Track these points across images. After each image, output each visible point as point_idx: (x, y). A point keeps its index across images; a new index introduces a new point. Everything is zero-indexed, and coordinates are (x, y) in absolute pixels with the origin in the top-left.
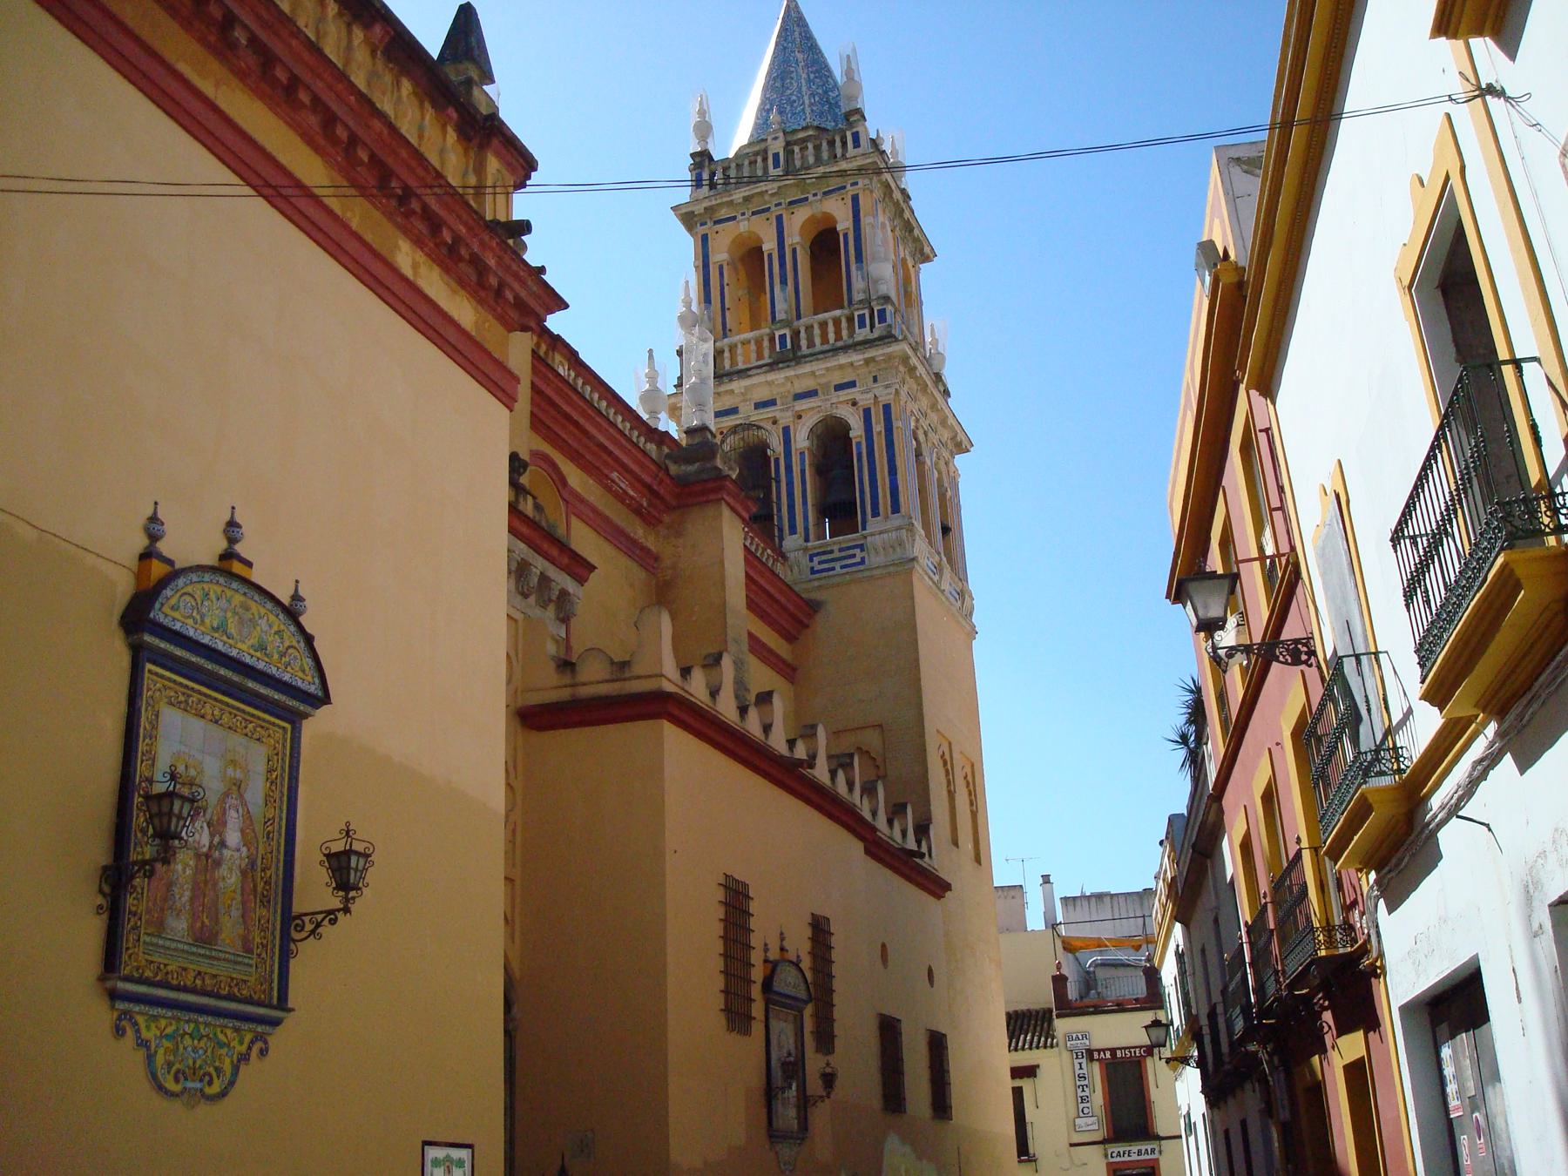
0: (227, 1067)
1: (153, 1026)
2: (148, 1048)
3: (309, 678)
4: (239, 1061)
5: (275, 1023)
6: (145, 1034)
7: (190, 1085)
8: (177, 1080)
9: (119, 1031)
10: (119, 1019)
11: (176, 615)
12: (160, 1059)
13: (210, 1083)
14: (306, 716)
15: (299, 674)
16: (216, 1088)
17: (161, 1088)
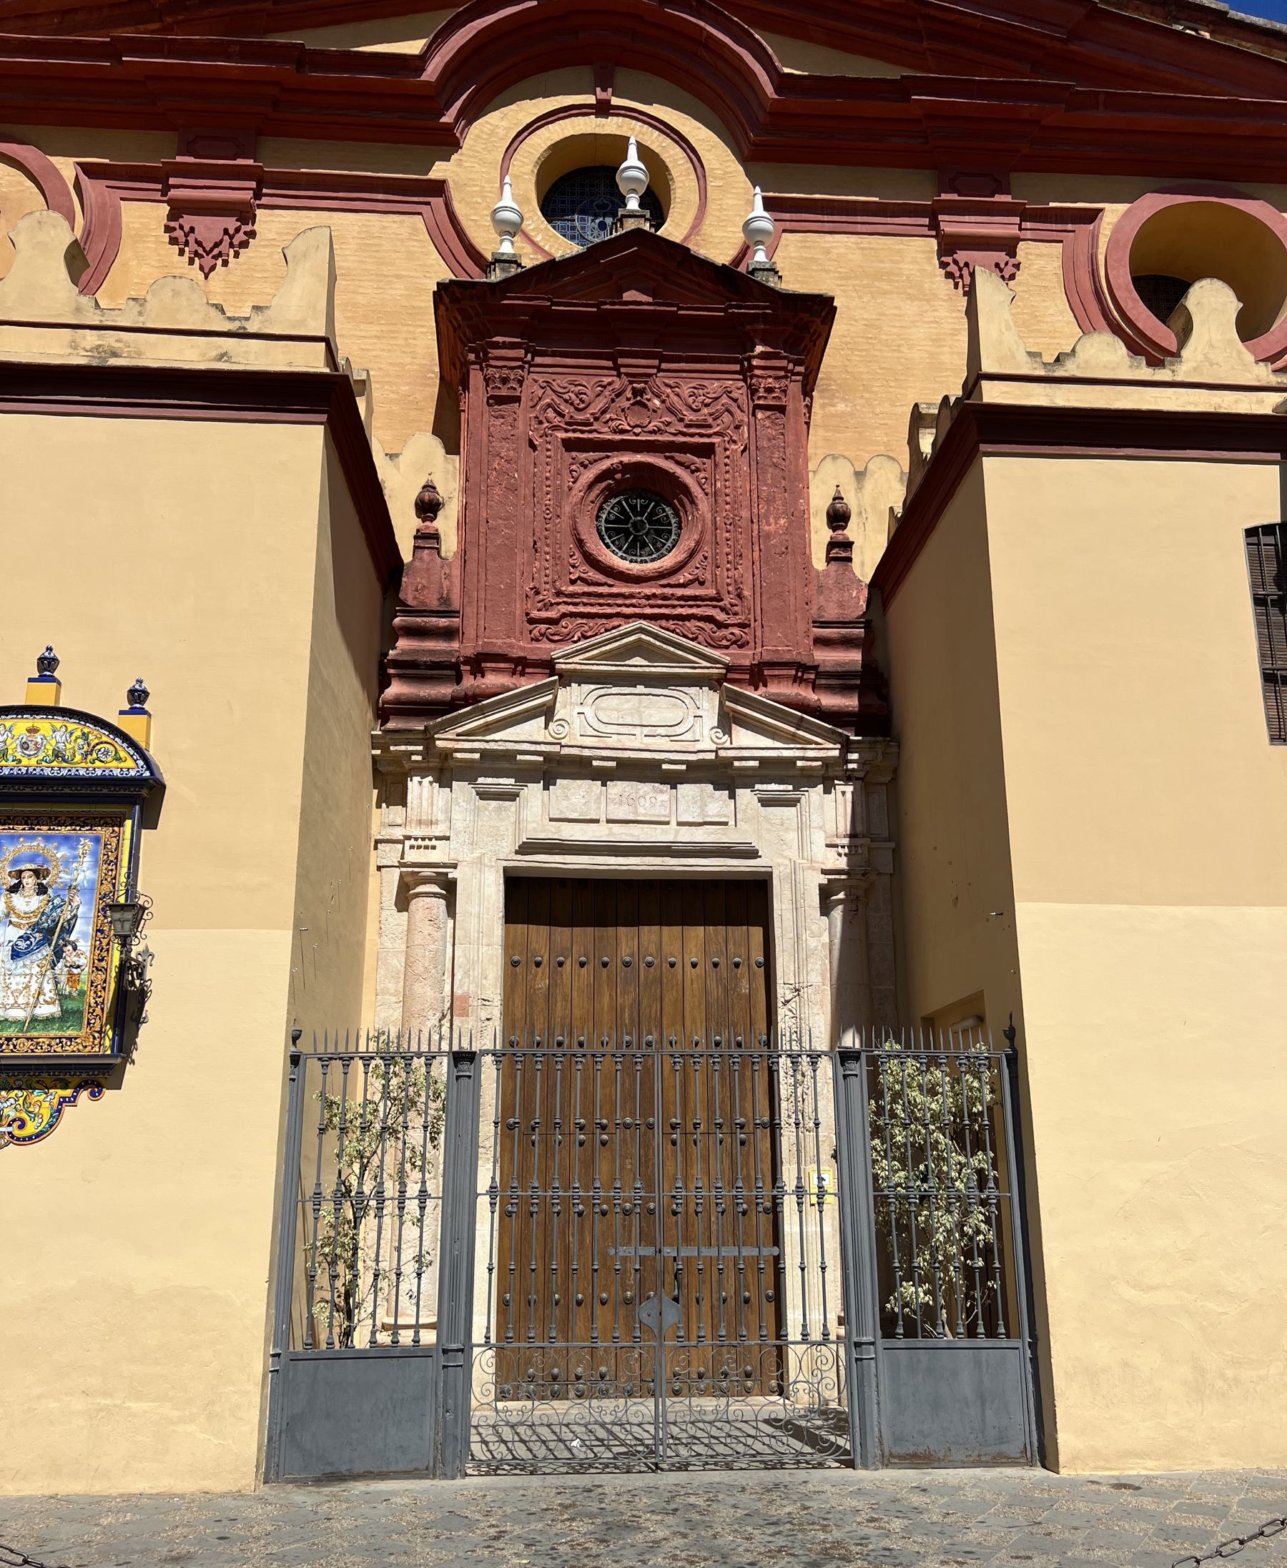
0: (46, 1113)
3: (130, 763)
4: (60, 1104)
13: (21, 1127)
16: (31, 1128)
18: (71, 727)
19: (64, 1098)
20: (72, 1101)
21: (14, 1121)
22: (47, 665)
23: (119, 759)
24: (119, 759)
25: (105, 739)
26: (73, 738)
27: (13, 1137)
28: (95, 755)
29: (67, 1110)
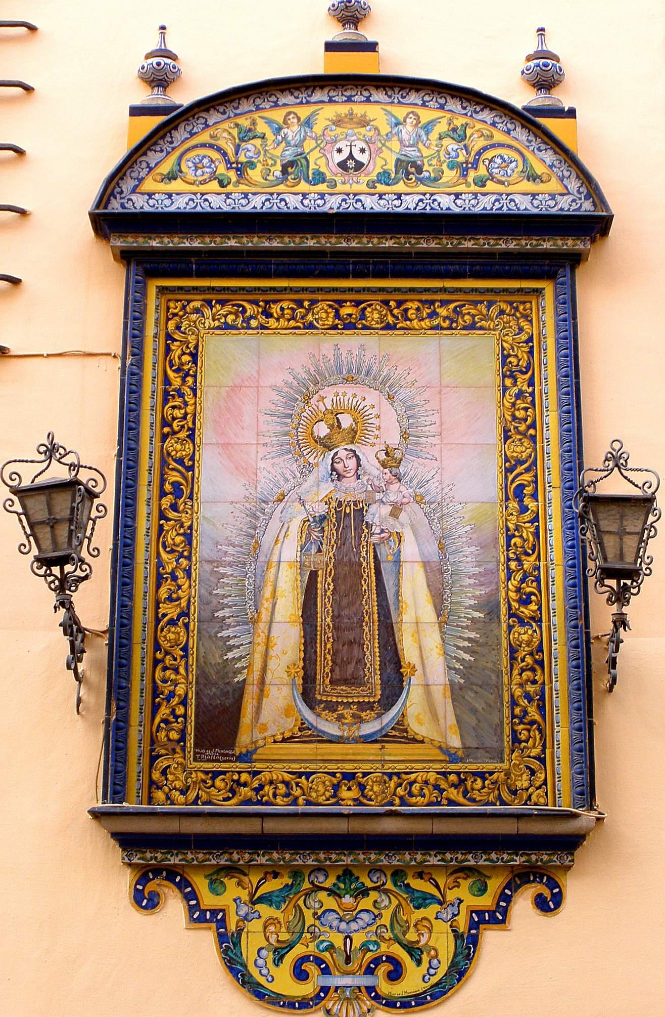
1: (230, 883)
2: (222, 923)
3: (554, 186)
4: (474, 925)
5: (570, 843)
6: (208, 900)
7: (336, 980)
8: (300, 974)
9: (146, 901)
10: (143, 879)
11: (176, 185)
12: (252, 944)
13: (396, 975)
14: (575, 259)
15: (555, 195)
16: (413, 981)
17: (258, 993)
18: (426, 115)
19: (480, 913)
20: (497, 916)
21: (377, 961)
22: (350, 15)
23: (533, 177)
24: (533, 177)
25: (499, 137)
26: (434, 136)
27: (377, 998)
28: (482, 171)
29: (490, 938)
